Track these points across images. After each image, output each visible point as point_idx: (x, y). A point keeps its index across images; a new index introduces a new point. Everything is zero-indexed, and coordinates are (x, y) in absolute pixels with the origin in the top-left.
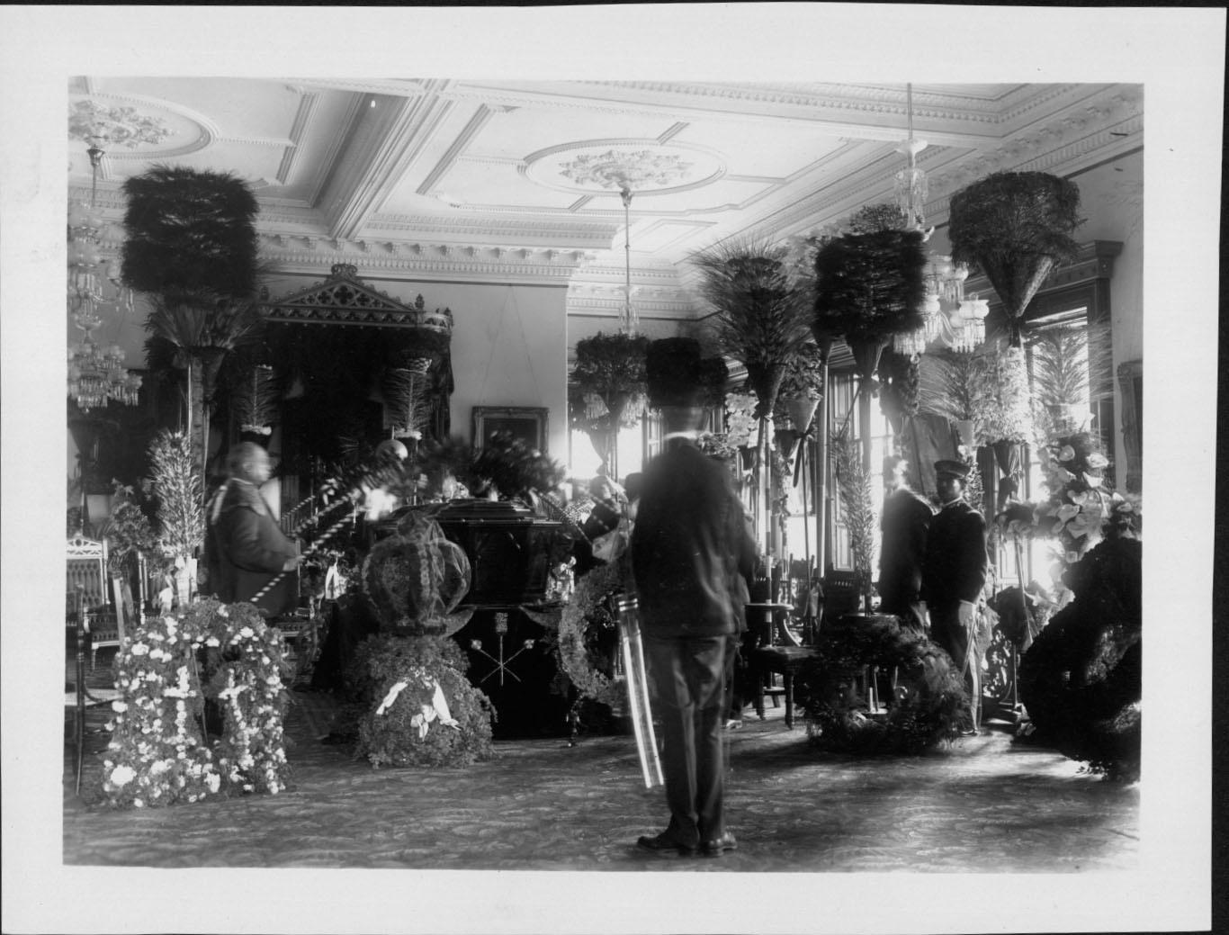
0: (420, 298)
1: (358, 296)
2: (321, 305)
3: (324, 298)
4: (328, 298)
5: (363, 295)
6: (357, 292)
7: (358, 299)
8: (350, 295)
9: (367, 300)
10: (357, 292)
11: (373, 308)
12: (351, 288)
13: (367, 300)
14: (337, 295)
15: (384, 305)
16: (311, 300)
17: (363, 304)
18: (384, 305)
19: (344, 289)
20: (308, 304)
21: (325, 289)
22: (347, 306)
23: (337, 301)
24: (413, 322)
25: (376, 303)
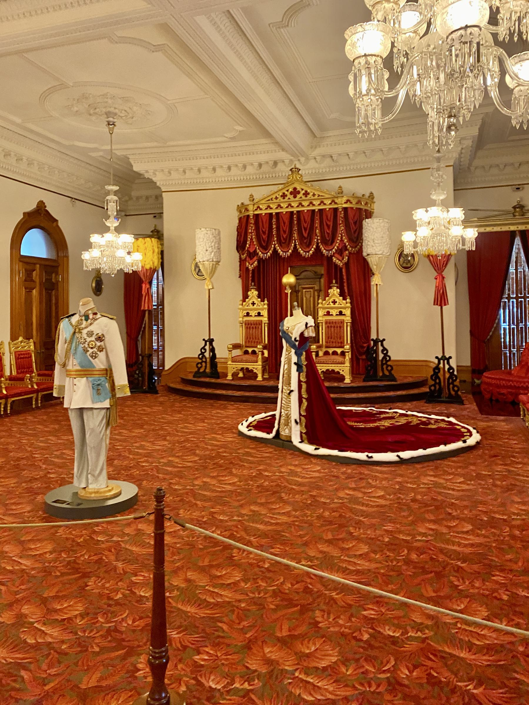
0: (340, 187)
1: (303, 192)
2: (282, 200)
3: (284, 196)
4: (286, 196)
5: (306, 191)
6: (302, 189)
7: (304, 194)
8: (299, 192)
9: (309, 194)
10: (302, 189)
11: (313, 198)
12: (299, 189)
13: (309, 194)
14: (291, 193)
15: (319, 196)
16: (276, 198)
17: (306, 197)
18: (319, 196)
19: (295, 189)
20: (275, 201)
21: (284, 191)
22: (297, 199)
23: (291, 197)
24: (336, 203)
25: (314, 195)
